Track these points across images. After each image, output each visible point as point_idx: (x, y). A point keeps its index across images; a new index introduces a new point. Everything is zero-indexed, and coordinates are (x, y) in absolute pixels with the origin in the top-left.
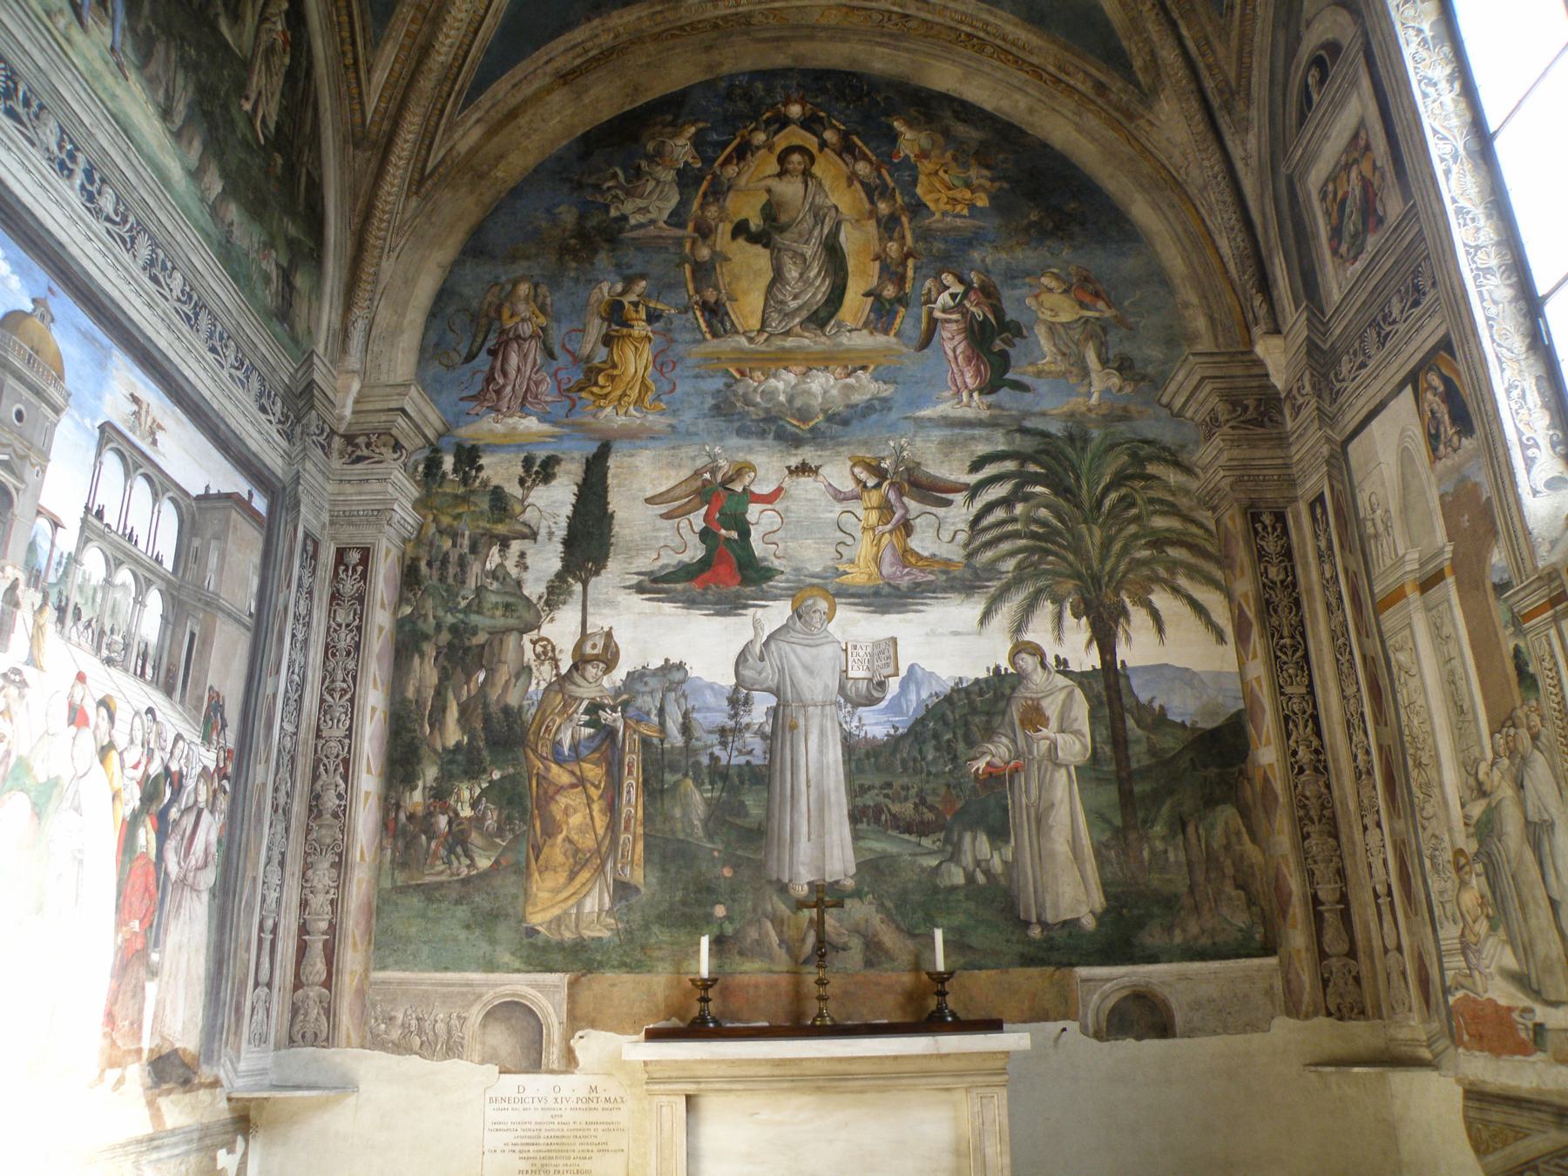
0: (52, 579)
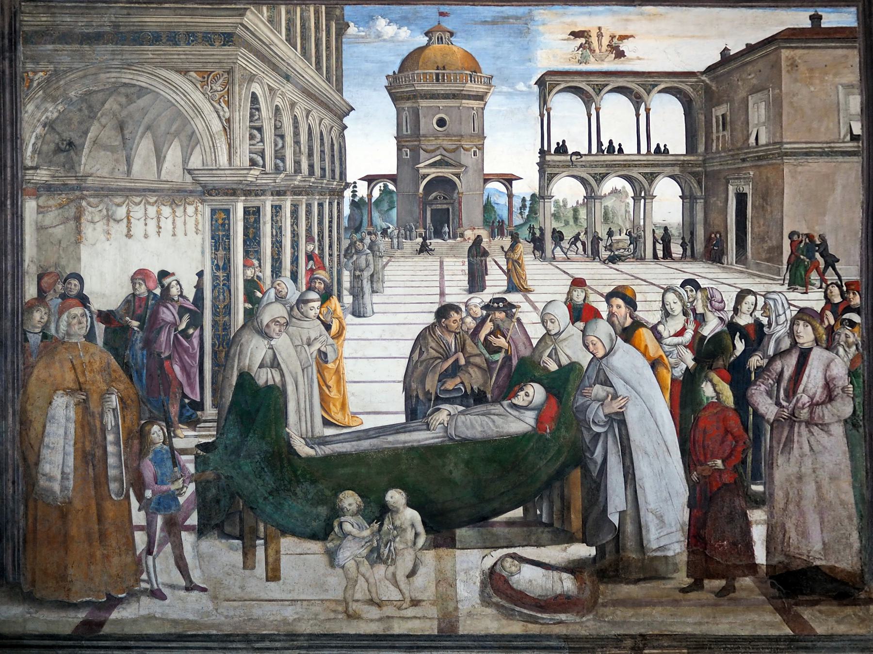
0: (517, 220)
